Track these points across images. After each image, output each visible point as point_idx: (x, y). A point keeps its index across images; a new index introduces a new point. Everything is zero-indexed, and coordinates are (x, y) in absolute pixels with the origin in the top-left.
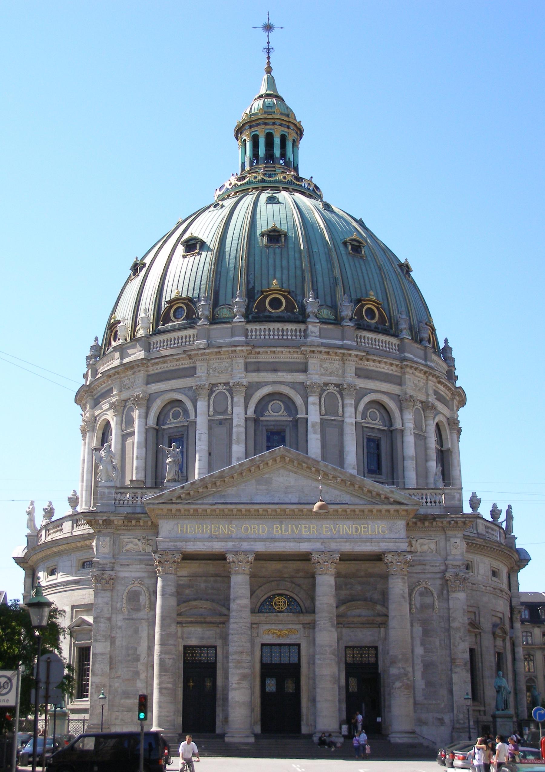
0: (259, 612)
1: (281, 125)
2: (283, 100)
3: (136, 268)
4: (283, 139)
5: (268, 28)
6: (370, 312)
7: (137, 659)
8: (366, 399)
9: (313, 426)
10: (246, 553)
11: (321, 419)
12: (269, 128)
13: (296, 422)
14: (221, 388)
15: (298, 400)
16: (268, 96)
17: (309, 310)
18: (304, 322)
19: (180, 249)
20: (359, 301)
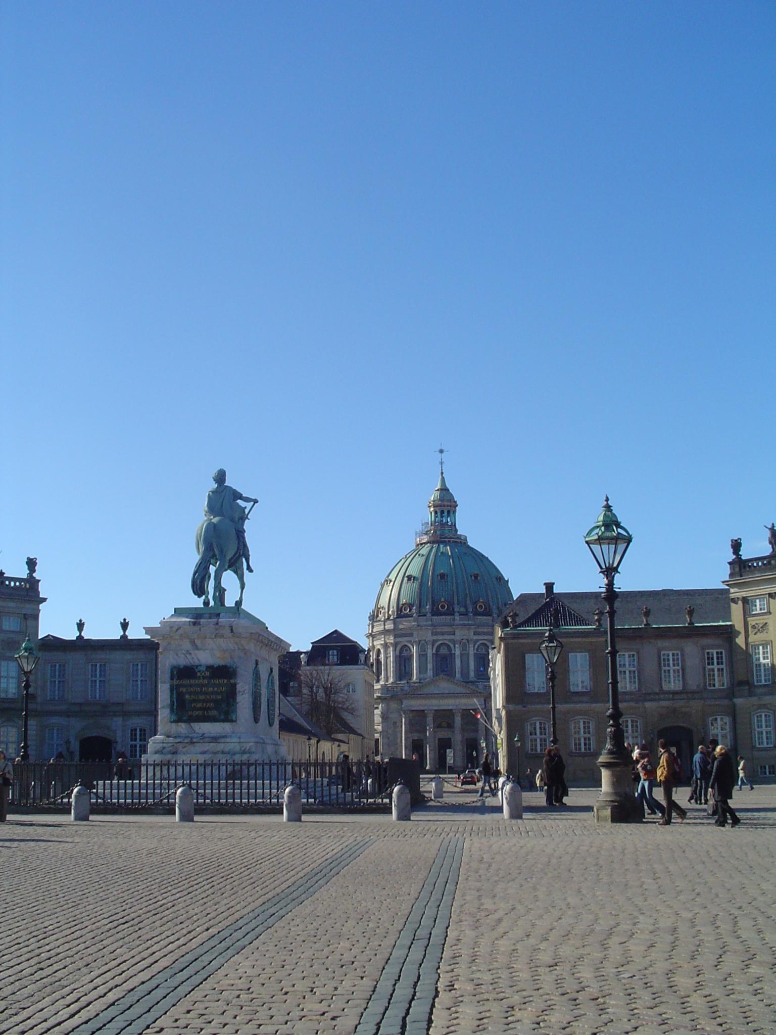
0: (438, 727)
1: (447, 506)
2: (448, 490)
3: (387, 581)
4: (449, 512)
5: (441, 451)
6: (481, 606)
7: (397, 744)
8: (478, 643)
9: (458, 656)
10: (431, 710)
11: (461, 653)
12: (442, 508)
13: (452, 654)
14: (423, 642)
15: (452, 646)
16: (441, 490)
17: (455, 610)
18: (453, 615)
19: (406, 579)
20: (475, 603)
